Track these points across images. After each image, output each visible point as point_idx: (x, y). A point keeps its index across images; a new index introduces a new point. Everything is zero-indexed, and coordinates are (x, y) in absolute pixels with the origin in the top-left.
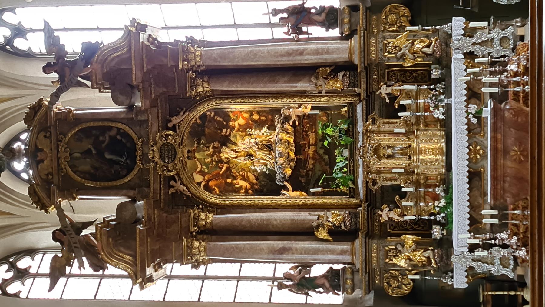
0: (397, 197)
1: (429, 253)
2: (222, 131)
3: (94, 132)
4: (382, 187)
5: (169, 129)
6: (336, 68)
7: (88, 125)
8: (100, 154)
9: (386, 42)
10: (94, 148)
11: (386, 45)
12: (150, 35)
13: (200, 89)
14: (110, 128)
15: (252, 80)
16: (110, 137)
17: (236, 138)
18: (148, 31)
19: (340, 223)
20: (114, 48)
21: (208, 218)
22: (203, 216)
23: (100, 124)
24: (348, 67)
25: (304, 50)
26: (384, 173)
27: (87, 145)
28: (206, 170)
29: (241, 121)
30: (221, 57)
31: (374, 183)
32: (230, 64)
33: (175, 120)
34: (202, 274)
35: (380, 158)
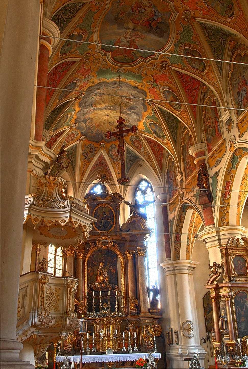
0: (90, 332)
1: (70, 345)
2: (109, 263)
3: (112, 216)
4: (94, 326)
5: (113, 243)
6: (138, 307)
7: (114, 214)
8: (104, 218)
9: (149, 326)
10: (106, 216)
11: (148, 326)
12: (147, 237)
13: (128, 255)
14: (113, 222)
15: (132, 274)
16: (110, 222)
17: (107, 268)
18: (149, 237)
19: (80, 308)
20: (144, 225)
21: (81, 257)
22: (82, 255)
23: (115, 219)
24: (139, 312)
25: (145, 294)
26: (100, 326)
27: (107, 213)
28: (94, 257)
29: (112, 270)
30: (141, 263)
31: (96, 322)
32: (139, 266)
33: (116, 246)
34: (57, 254)
35: (106, 325)
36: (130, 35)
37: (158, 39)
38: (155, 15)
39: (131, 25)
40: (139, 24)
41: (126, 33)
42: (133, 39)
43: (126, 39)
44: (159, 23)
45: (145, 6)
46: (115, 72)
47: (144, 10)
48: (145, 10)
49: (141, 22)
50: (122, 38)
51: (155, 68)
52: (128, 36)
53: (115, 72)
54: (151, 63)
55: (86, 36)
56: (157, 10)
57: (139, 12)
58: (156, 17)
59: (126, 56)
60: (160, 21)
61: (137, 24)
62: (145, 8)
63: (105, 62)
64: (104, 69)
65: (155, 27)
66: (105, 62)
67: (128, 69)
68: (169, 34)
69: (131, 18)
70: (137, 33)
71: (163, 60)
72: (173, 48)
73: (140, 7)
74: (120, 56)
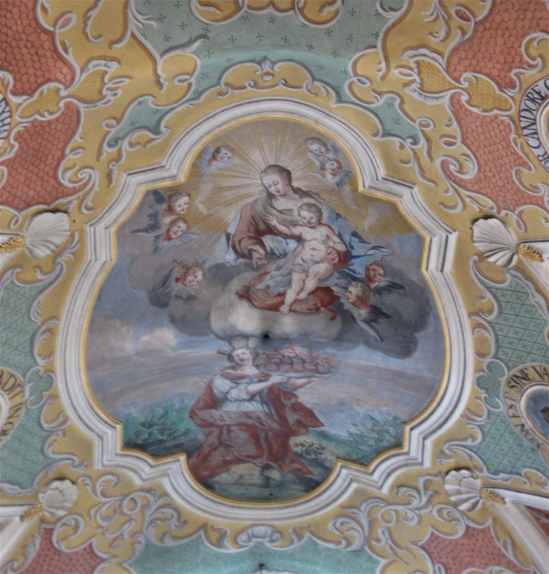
36: (257, 366)
37: (395, 364)
38: (346, 257)
39: (246, 319)
40: (284, 308)
41: (230, 358)
42: (276, 379)
43: (242, 387)
44: (379, 291)
45: (295, 224)
46: (232, 550)
47: (292, 244)
48: (299, 239)
49: (290, 297)
50: (221, 385)
51: (426, 506)
52: (250, 370)
53: (232, 550)
54: (398, 485)
55: (18, 400)
56: (354, 234)
57: (271, 255)
58: (358, 267)
59: (266, 467)
60: (381, 282)
61: (275, 308)
62: (297, 231)
63: (162, 507)
64: (170, 543)
65: (363, 313)
66: (162, 507)
67: (294, 530)
68: (439, 336)
69: (236, 285)
70: (288, 352)
71: (451, 462)
72: (475, 397)
73: (271, 231)
74: (238, 469)
